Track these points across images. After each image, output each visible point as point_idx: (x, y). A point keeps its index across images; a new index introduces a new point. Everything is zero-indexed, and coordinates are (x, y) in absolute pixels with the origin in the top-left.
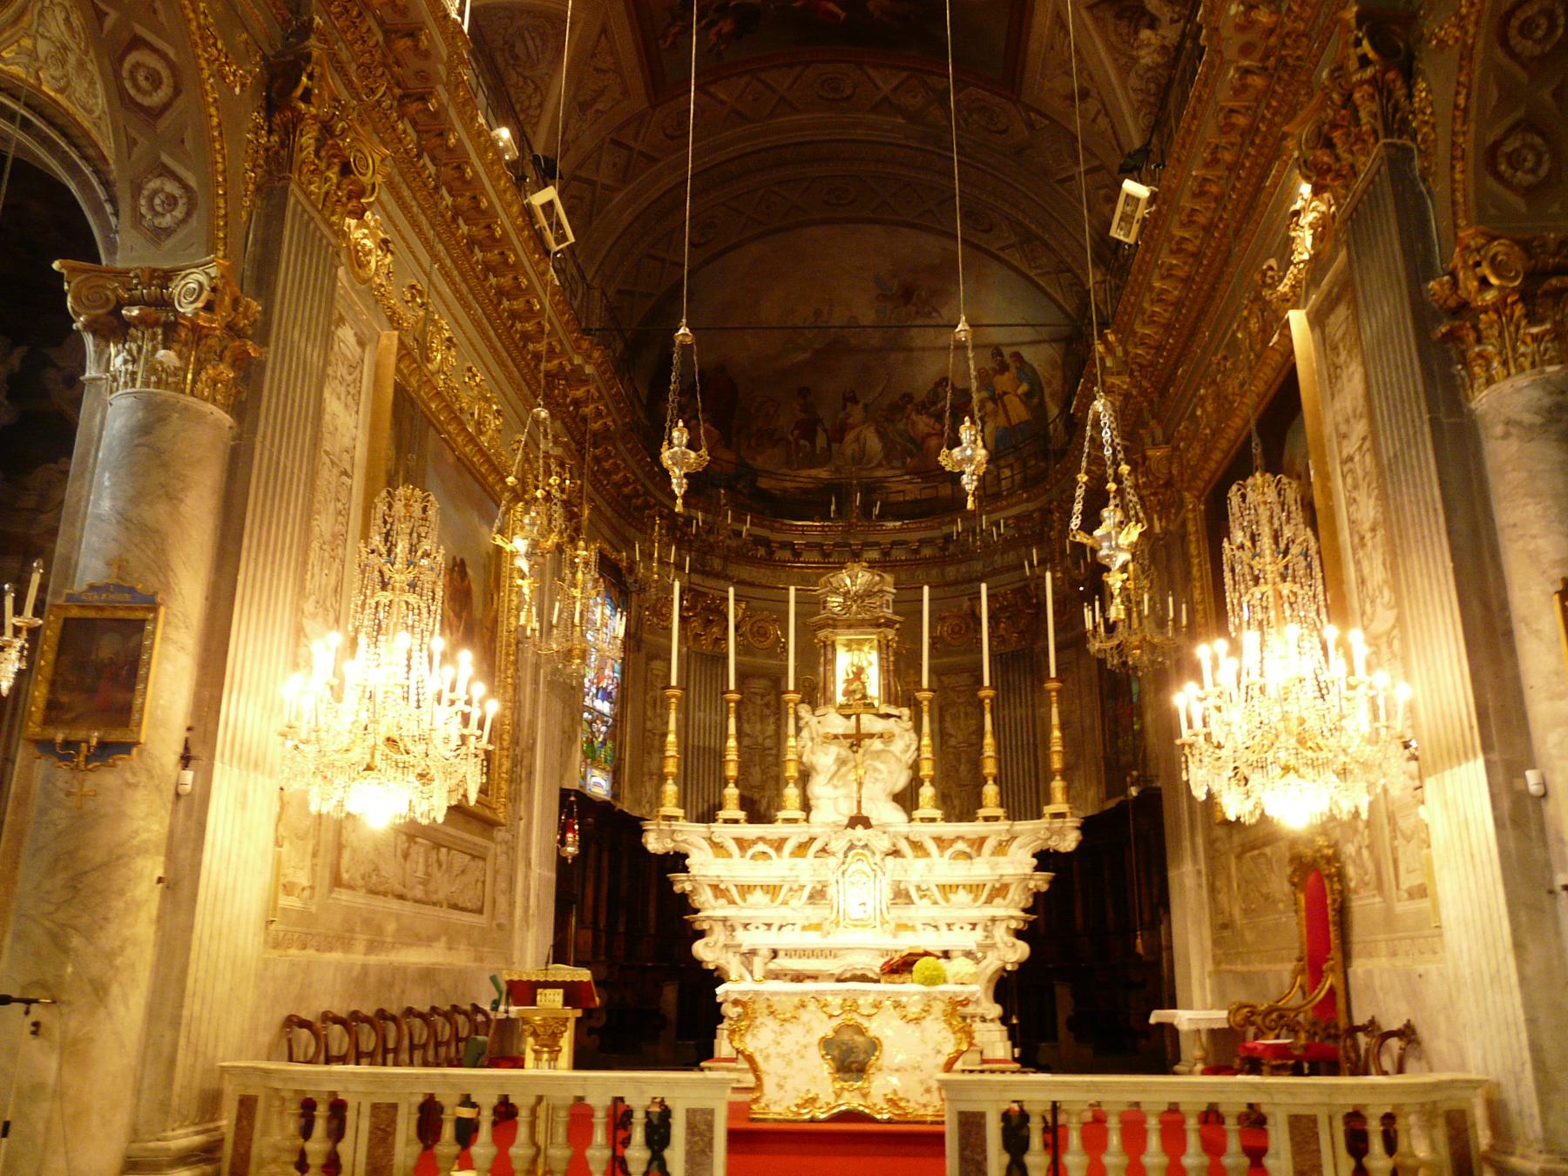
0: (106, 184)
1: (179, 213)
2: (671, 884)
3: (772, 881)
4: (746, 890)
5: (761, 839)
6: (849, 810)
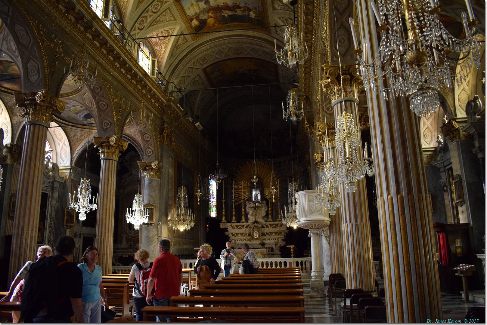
0: (142, 151)
1: (151, 153)
2: (225, 233)
3: (241, 233)
4: (237, 234)
5: (240, 225)
6: (254, 220)
